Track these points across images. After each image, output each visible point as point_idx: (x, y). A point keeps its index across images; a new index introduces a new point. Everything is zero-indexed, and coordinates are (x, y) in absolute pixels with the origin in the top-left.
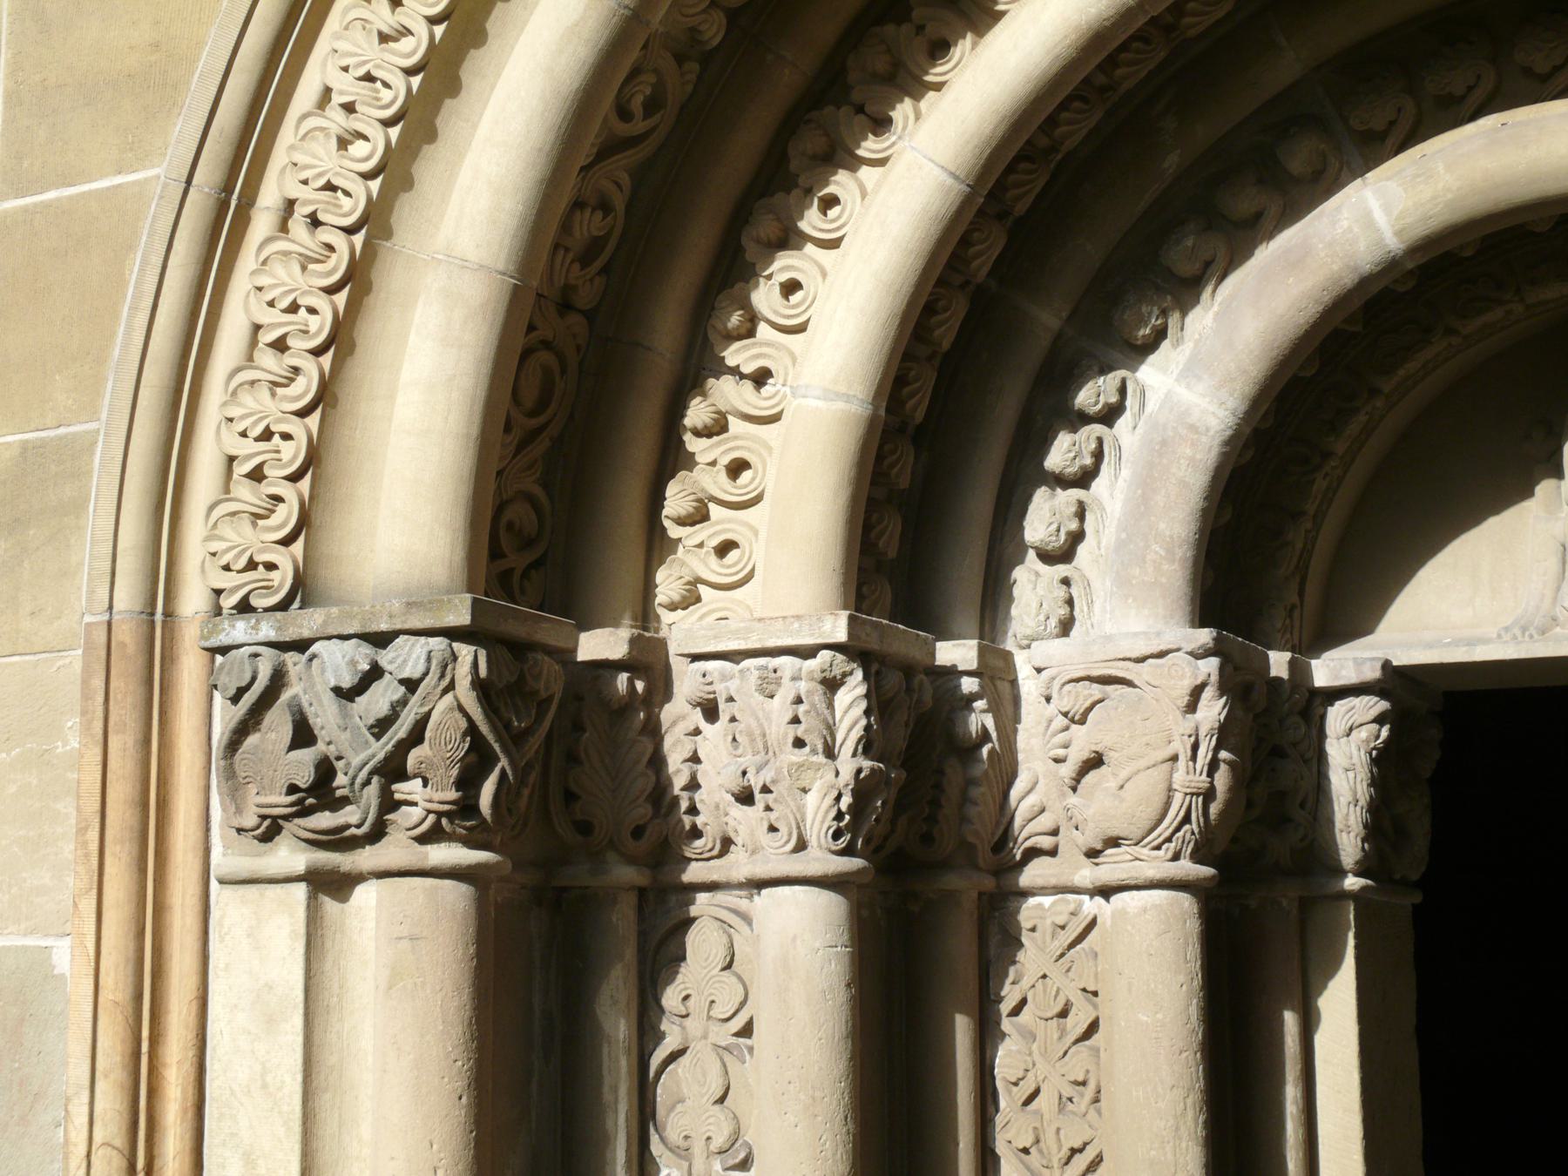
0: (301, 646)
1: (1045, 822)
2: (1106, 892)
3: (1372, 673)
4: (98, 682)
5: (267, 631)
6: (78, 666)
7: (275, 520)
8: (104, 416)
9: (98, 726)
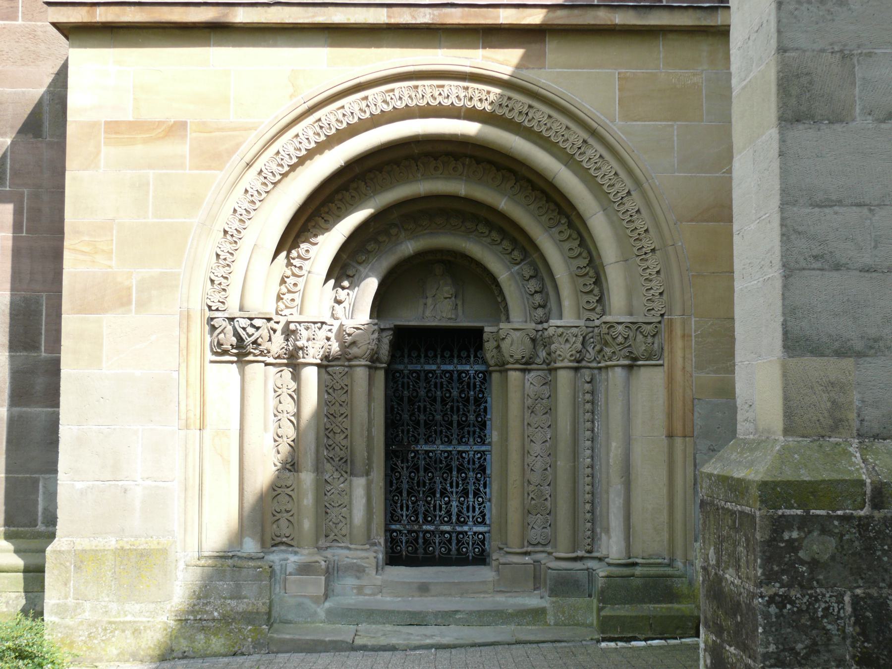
2: (350, 366)
3: (392, 326)
9: (185, 330)
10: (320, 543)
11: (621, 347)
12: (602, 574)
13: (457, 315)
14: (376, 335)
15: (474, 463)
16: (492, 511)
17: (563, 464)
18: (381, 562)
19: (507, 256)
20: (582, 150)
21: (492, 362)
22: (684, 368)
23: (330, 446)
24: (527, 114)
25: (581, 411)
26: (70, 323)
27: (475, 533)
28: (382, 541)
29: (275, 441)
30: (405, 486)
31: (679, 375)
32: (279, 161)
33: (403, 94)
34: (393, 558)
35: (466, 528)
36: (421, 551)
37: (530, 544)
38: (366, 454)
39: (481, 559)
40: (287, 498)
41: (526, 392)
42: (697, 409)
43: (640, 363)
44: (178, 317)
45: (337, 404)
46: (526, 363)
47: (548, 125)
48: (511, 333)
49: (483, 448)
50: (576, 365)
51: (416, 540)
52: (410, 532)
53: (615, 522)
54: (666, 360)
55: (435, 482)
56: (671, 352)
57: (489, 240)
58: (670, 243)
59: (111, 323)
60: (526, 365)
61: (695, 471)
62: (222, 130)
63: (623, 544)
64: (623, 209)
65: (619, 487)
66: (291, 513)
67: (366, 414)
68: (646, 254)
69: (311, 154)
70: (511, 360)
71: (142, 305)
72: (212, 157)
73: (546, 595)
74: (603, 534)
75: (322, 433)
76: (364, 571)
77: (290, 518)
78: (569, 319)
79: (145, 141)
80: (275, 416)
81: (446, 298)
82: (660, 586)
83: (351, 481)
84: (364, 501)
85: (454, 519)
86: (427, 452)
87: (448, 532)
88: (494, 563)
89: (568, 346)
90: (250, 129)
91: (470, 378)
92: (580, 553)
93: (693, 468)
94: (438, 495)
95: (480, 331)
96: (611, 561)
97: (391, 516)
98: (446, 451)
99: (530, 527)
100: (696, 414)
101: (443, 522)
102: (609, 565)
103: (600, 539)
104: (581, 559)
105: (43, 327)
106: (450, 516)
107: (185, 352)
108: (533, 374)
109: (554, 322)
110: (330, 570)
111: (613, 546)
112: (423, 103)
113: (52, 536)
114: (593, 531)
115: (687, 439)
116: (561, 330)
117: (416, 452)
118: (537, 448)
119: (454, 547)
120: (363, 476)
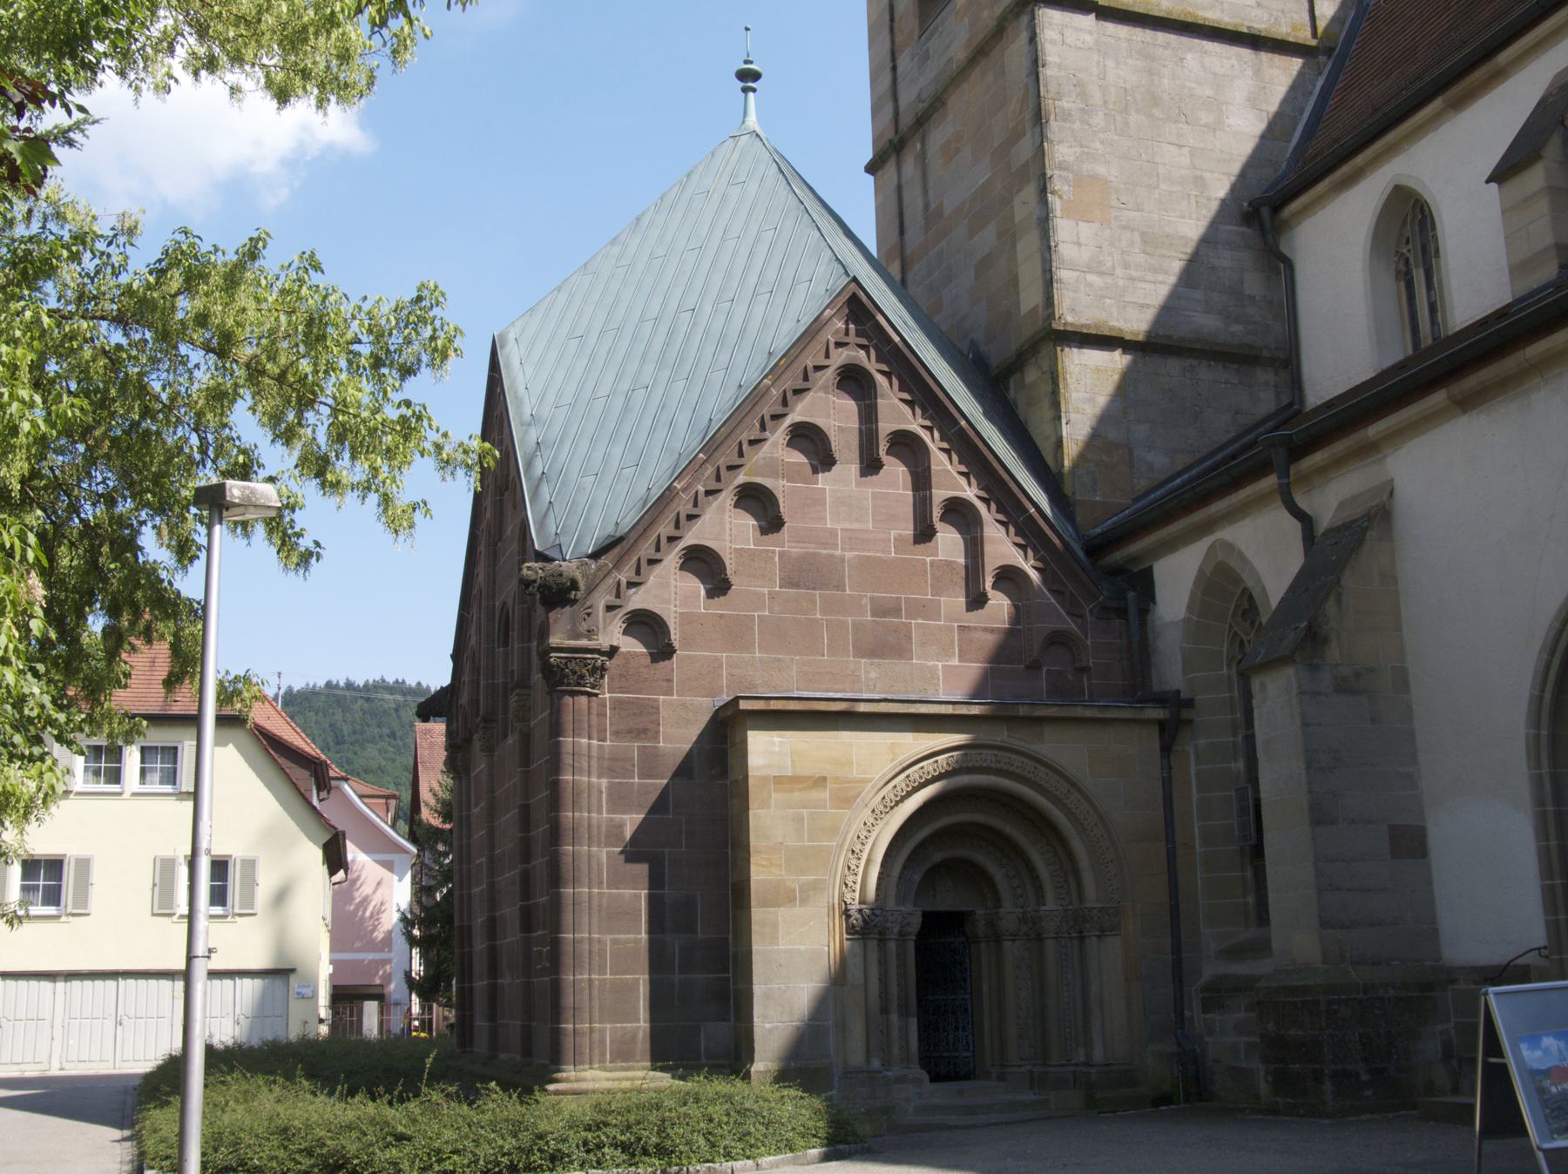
26: (757, 914)
48: (1009, 912)
59: (783, 913)
69: (903, 798)
71: (803, 902)
95: (971, 913)
113: (752, 1061)
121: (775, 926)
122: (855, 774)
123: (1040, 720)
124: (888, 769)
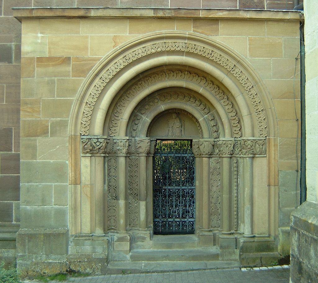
0: (91, 139)
1: (135, 151)
4: (70, 140)
5: (88, 137)
6: (68, 139)
7: (86, 128)
8: (70, 118)
9: (71, 144)
10: (127, 228)
11: (250, 149)
12: (242, 241)
13: (182, 135)
14: (149, 144)
15: (189, 194)
16: (197, 214)
17: (225, 196)
18: (152, 234)
19: (203, 111)
20: (234, 69)
21: (196, 154)
22: (275, 158)
23: (131, 188)
24: (211, 54)
25: (233, 175)
27: (189, 221)
28: (152, 225)
29: (108, 187)
30: (160, 204)
31: (273, 161)
32: (109, 73)
33: (160, 46)
34: (156, 233)
35: (186, 220)
36: (167, 229)
37: (212, 227)
38: (145, 192)
39: (192, 232)
40: (114, 211)
41: (210, 166)
42: (280, 175)
43: (257, 156)
44: (68, 138)
45: (133, 172)
46: (210, 155)
47: (220, 59)
48: (203, 142)
49: (193, 187)
50: (230, 156)
51: (165, 225)
52: (163, 222)
53: (247, 220)
54: (267, 155)
55: (173, 201)
56: (269, 151)
57: (195, 104)
58: (269, 107)
59: (39, 141)
60: (210, 155)
61: (279, 199)
62: (85, 60)
63: (250, 229)
64: (250, 93)
65: (248, 206)
66: (115, 217)
67: (145, 176)
68: (259, 112)
70: (204, 154)
71: (53, 134)
72: (81, 71)
73: (219, 248)
74: (242, 224)
75: (128, 184)
76: (145, 239)
77: (115, 219)
78: (228, 137)
79: (53, 65)
80: (108, 177)
81: (177, 128)
82: (266, 246)
83: (139, 203)
84: (145, 211)
85: (181, 215)
86: (169, 190)
87: (178, 221)
88: (197, 234)
89: (227, 148)
90: (97, 60)
91: (187, 159)
92: (232, 231)
93: (278, 198)
94: (174, 207)
96: (245, 236)
97: (155, 216)
98: (177, 189)
99: (212, 220)
100: (279, 177)
101: (176, 218)
102: (244, 237)
103: (240, 226)
104: (233, 234)
105: (13, 141)
106: (179, 215)
107: (71, 153)
108: (213, 159)
109: (221, 139)
110: (132, 239)
111: (245, 229)
112: (168, 49)
114: (238, 222)
115: (276, 187)
116: (224, 142)
117: (165, 190)
118: (214, 189)
119: (181, 227)
120: (144, 201)
121: (34, 148)
122: (89, 55)
123: (216, 20)
124: (110, 52)
